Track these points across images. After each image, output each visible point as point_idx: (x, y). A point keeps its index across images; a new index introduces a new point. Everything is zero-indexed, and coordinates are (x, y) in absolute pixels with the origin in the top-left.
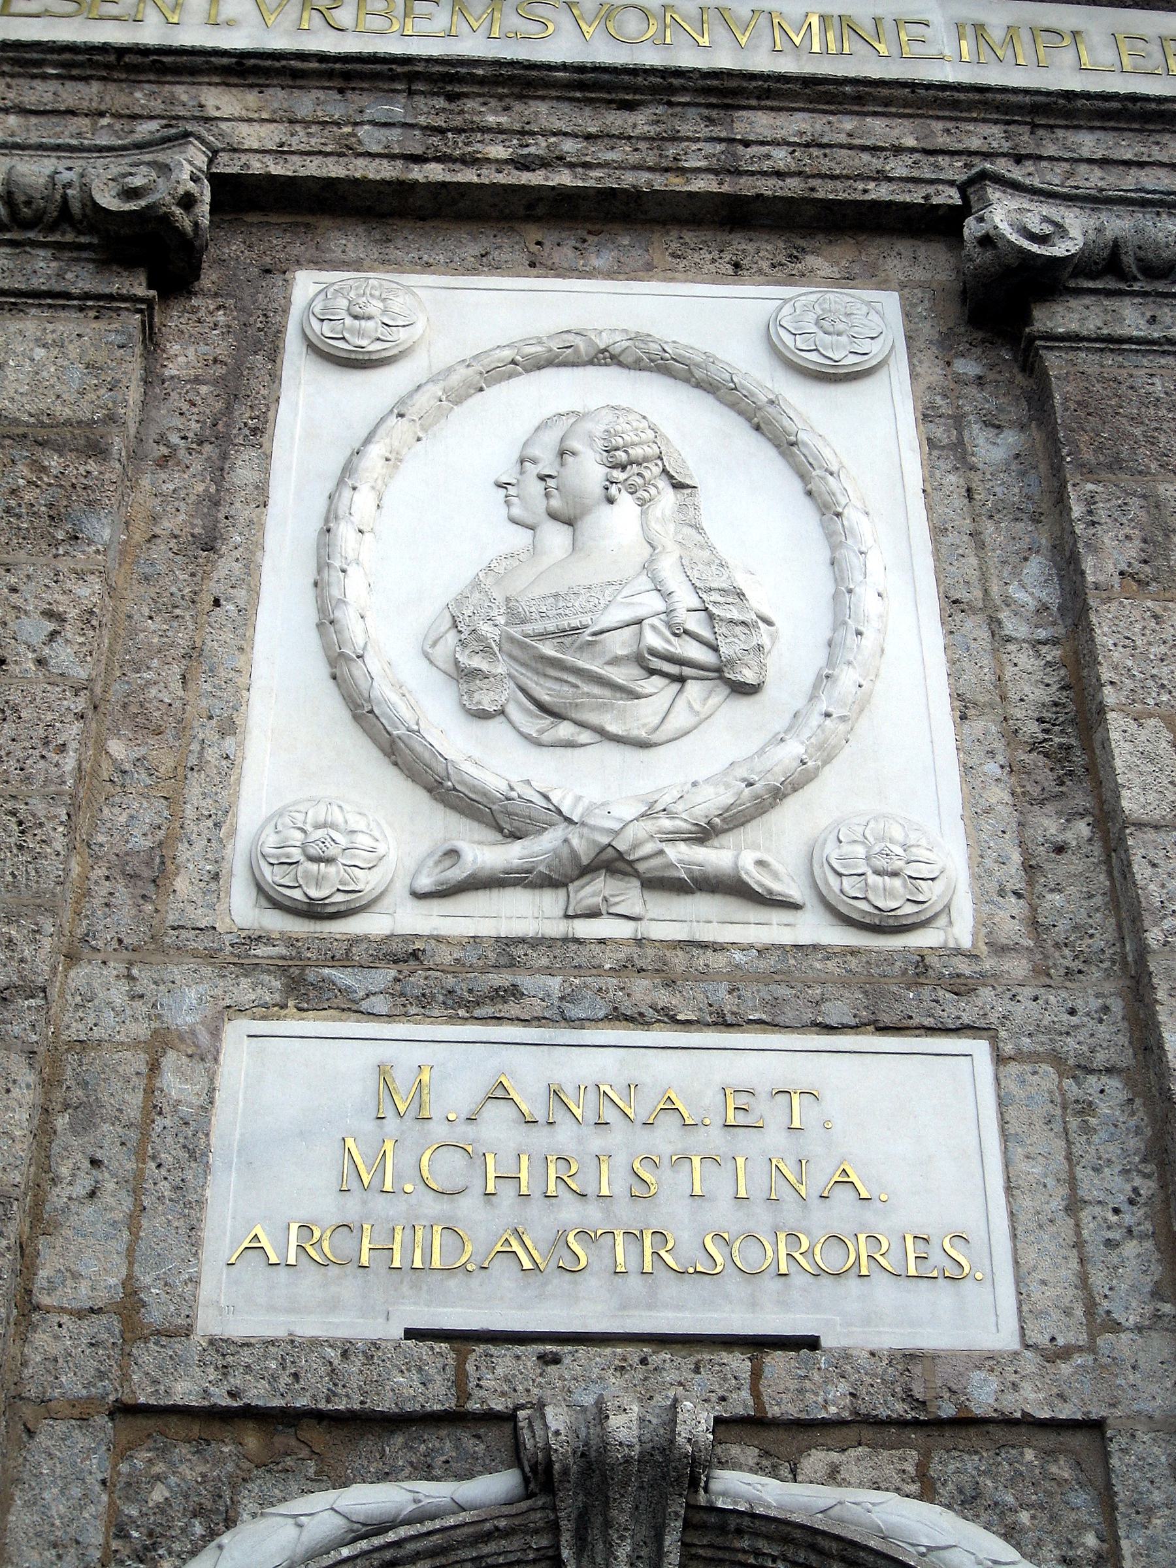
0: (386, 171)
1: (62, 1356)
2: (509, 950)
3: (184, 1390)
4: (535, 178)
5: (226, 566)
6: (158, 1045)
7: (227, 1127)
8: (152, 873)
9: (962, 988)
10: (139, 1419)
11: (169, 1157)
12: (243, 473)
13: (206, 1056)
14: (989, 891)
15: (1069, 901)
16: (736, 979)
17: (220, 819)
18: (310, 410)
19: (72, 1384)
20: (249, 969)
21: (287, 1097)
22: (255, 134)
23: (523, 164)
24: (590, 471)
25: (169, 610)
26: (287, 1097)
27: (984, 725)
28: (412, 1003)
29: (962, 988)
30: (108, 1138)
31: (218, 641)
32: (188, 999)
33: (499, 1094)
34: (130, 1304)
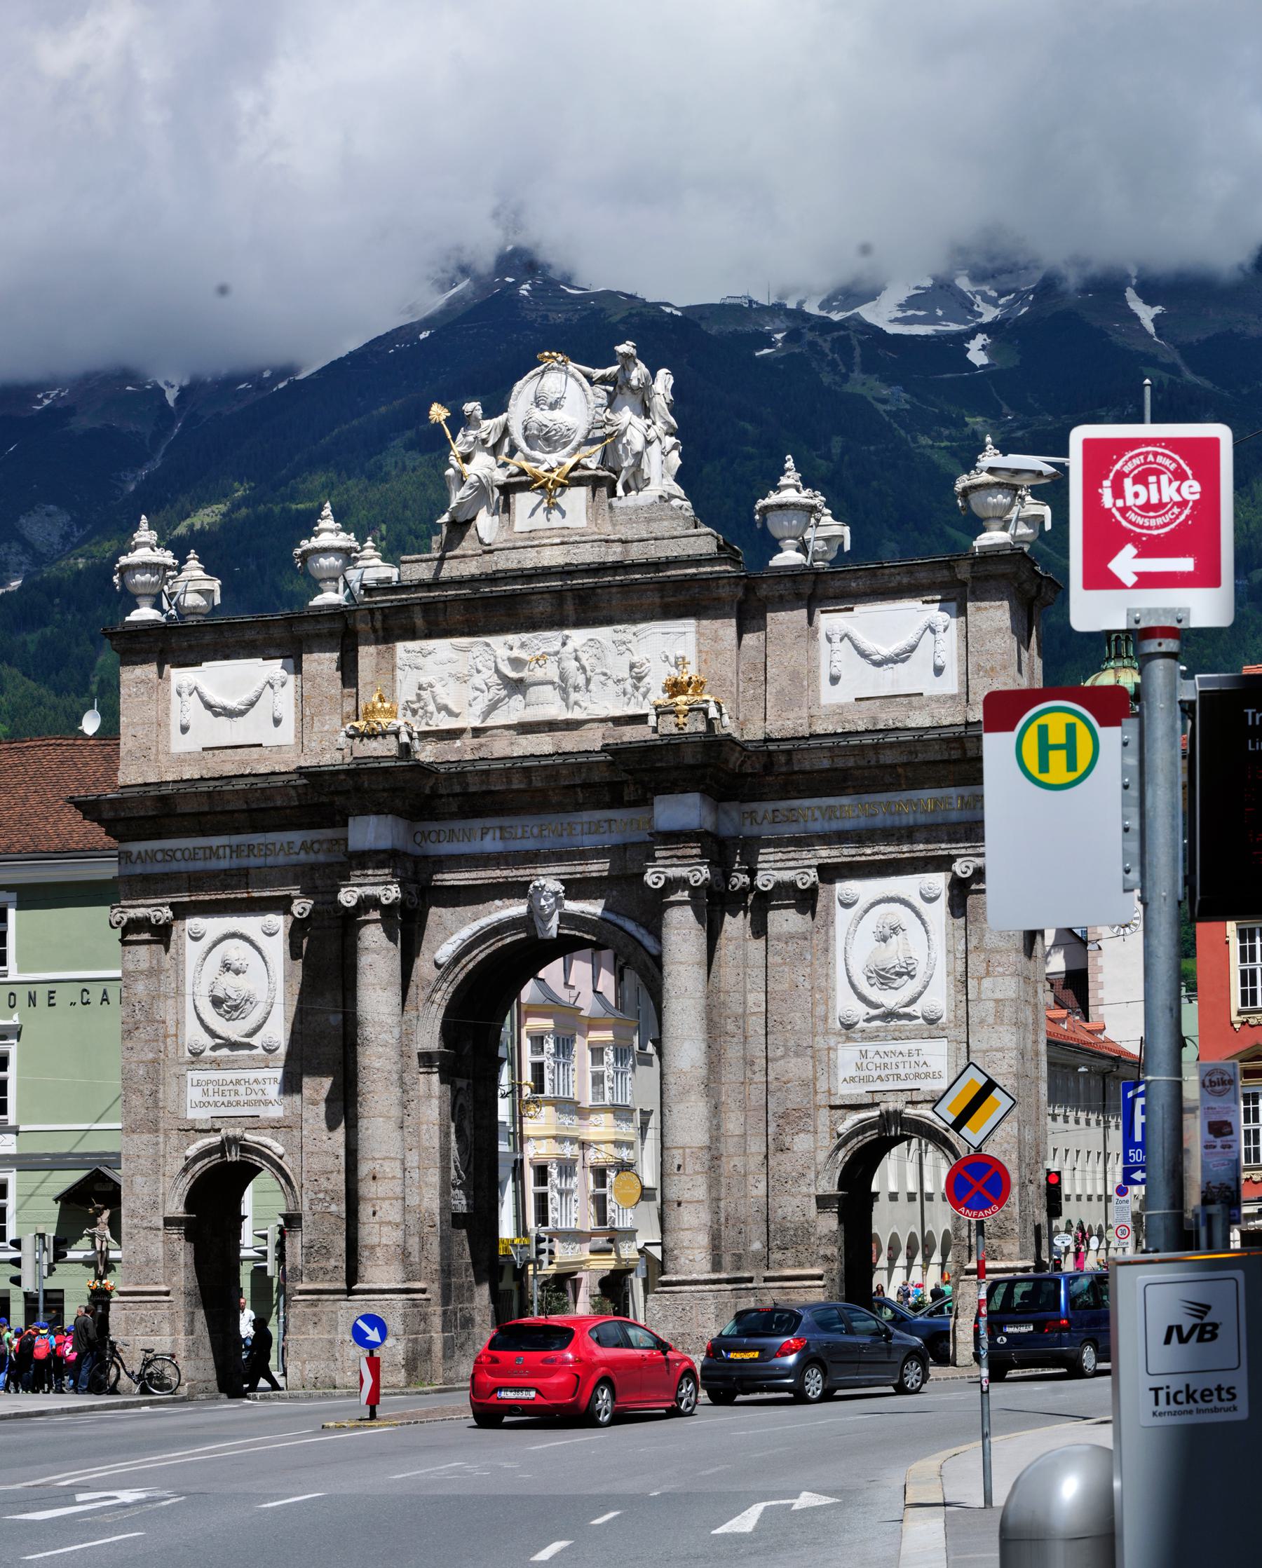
0: (849, 859)
1: (822, 1099)
2: (878, 1029)
3: (838, 1102)
4: (877, 857)
5: (831, 955)
6: (829, 1049)
7: (839, 1061)
8: (826, 1019)
9: (943, 1029)
10: (832, 1107)
11: (831, 1068)
12: (831, 933)
13: (836, 1050)
14: (949, 1010)
15: (962, 1012)
16: (910, 1031)
17: (834, 1008)
18: (842, 917)
19: (823, 1103)
20: (841, 1035)
21: (847, 1055)
22: (826, 854)
23: (873, 854)
24: (887, 931)
25: (821, 966)
26: (847, 1055)
27: (951, 977)
28: (864, 1039)
29: (943, 1029)
30: (823, 1065)
31: (831, 972)
32: (832, 1041)
33: (877, 1053)
34: (829, 1091)
